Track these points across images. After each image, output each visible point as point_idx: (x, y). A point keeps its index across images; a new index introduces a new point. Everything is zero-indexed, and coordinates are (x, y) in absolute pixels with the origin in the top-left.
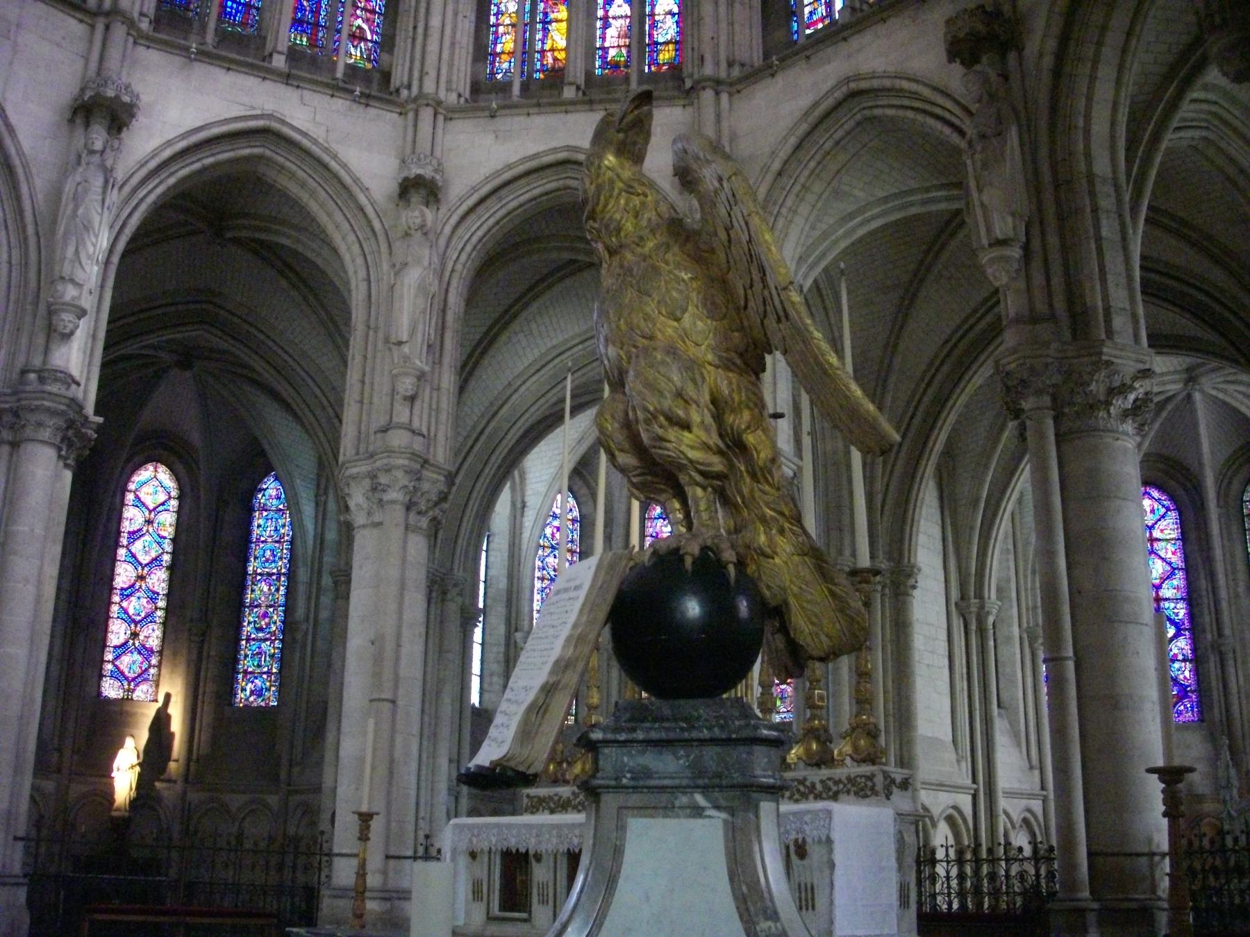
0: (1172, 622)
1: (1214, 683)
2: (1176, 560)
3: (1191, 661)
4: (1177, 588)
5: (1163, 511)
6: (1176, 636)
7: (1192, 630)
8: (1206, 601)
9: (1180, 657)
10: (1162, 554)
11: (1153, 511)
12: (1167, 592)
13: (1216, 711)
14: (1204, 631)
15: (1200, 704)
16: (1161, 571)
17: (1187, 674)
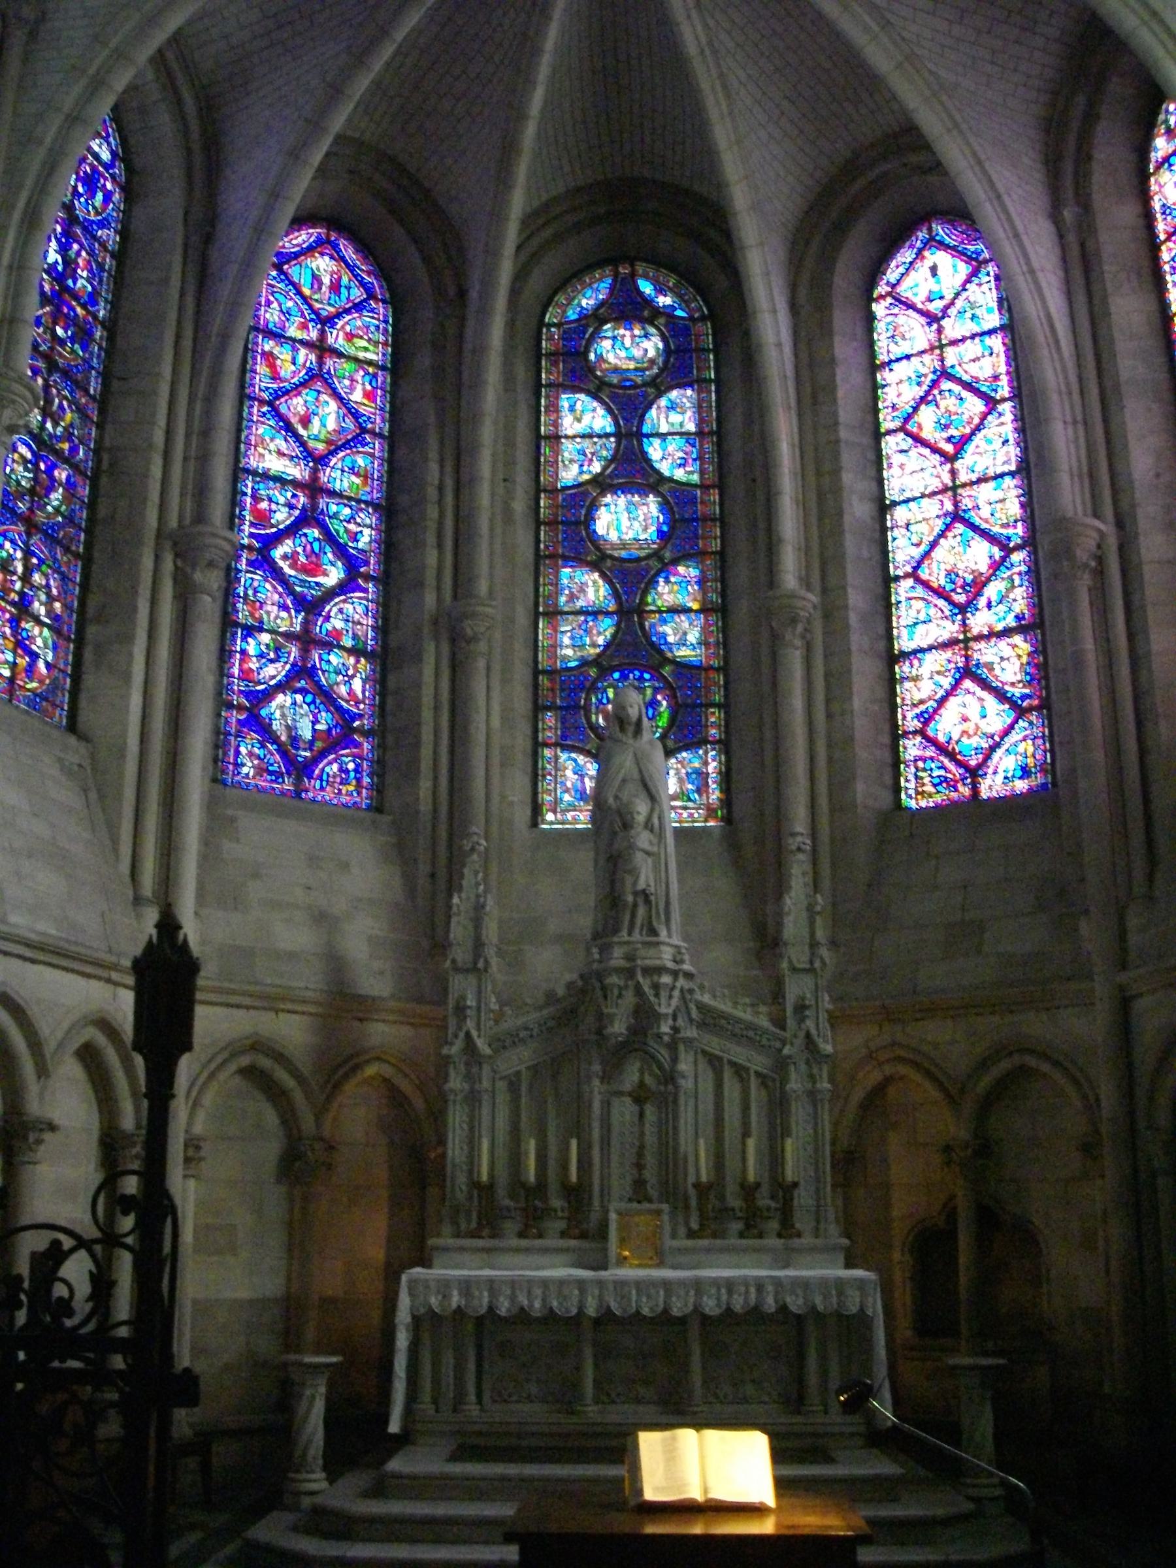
0: (341, 551)
1: (427, 715)
2: (374, 413)
3: (370, 656)
4: (366, 476)
5: (357, 294)
6: (344, 588)
7: (385, 580)
8: (433, 512)
9: (347, 642)
10: (342, 386)
11: (336, 287)
12: (337, 477)
13: (425, 785)
14: (420, 584)
15: (380, 768)
16: (331, 425)
17: (357, 684)
